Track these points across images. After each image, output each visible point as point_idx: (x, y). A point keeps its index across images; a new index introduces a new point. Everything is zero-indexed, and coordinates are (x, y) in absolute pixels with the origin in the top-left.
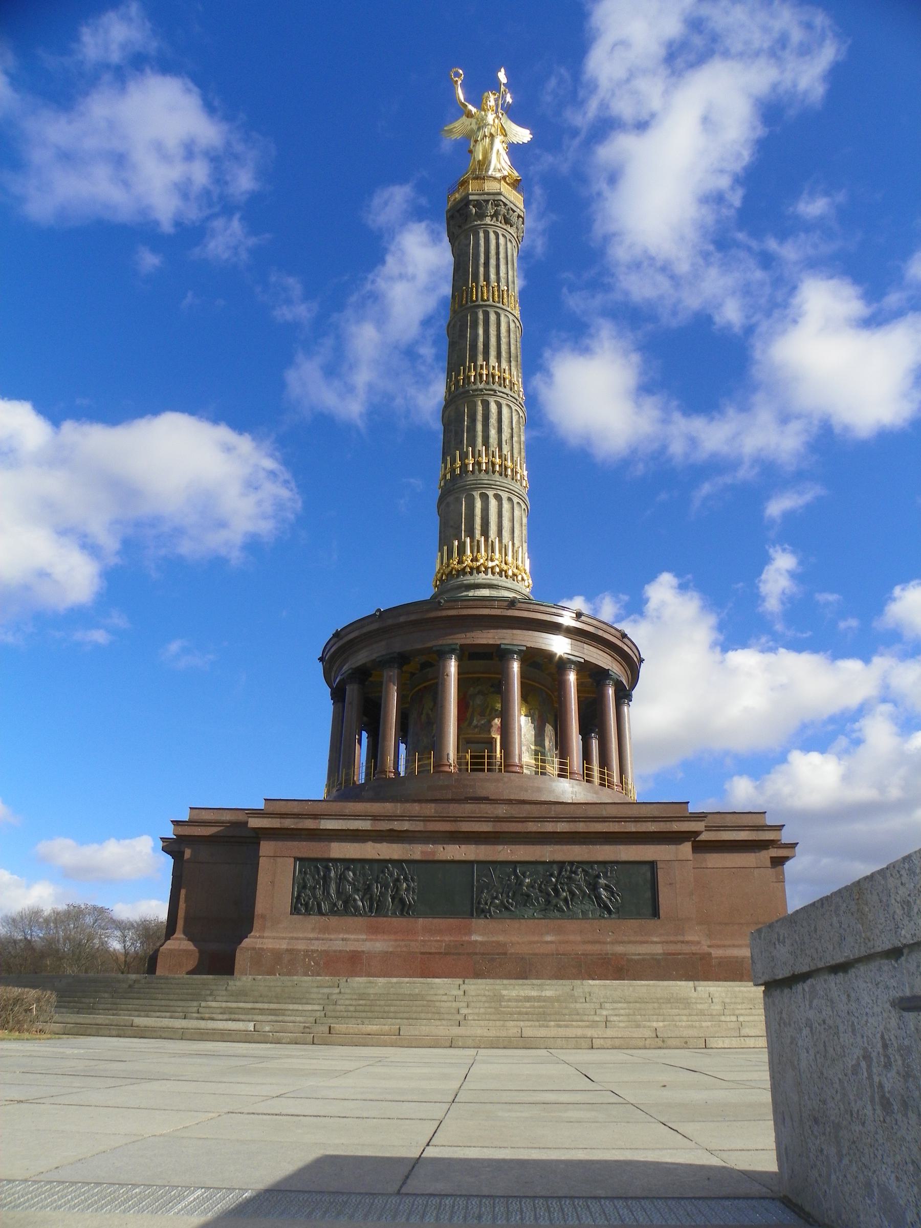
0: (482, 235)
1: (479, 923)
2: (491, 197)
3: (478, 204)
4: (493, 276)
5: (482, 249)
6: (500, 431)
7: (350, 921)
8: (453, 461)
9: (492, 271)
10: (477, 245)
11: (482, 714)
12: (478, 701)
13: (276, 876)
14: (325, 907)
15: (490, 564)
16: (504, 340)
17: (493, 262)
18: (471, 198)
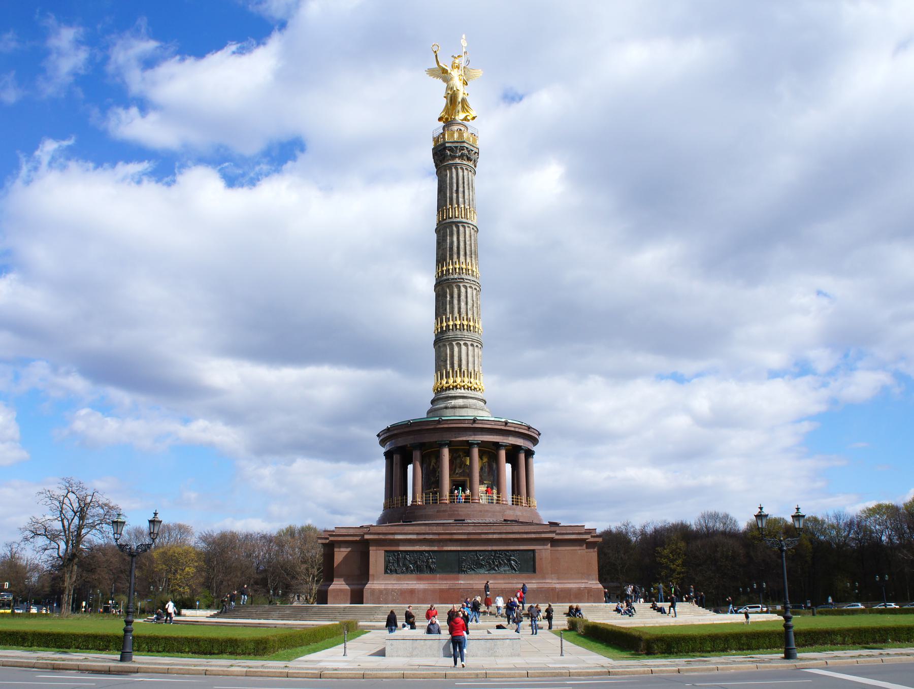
0: (454, 170)
1: (462, 576)
2: (459, 145)
3: (451, 149)
4: (461, 200)
5: (455, 181)
6: (467, 304)
7: (409, 576)
8: (442, 322)
9: (461, 195)
10: (451, 178)
11: (460, 467)
12: (458, 461)
13: (377, 558)
14: (399, 571)
15: (462, 384)
16: (468, 243)
17: (461, 189)
18: (447, 145)
